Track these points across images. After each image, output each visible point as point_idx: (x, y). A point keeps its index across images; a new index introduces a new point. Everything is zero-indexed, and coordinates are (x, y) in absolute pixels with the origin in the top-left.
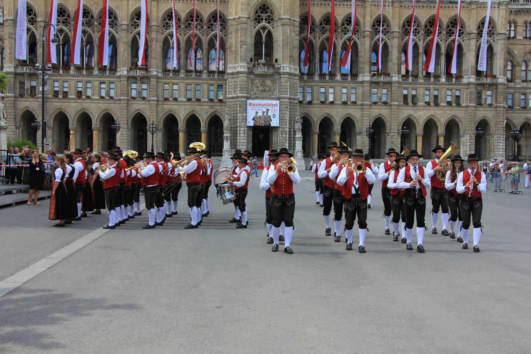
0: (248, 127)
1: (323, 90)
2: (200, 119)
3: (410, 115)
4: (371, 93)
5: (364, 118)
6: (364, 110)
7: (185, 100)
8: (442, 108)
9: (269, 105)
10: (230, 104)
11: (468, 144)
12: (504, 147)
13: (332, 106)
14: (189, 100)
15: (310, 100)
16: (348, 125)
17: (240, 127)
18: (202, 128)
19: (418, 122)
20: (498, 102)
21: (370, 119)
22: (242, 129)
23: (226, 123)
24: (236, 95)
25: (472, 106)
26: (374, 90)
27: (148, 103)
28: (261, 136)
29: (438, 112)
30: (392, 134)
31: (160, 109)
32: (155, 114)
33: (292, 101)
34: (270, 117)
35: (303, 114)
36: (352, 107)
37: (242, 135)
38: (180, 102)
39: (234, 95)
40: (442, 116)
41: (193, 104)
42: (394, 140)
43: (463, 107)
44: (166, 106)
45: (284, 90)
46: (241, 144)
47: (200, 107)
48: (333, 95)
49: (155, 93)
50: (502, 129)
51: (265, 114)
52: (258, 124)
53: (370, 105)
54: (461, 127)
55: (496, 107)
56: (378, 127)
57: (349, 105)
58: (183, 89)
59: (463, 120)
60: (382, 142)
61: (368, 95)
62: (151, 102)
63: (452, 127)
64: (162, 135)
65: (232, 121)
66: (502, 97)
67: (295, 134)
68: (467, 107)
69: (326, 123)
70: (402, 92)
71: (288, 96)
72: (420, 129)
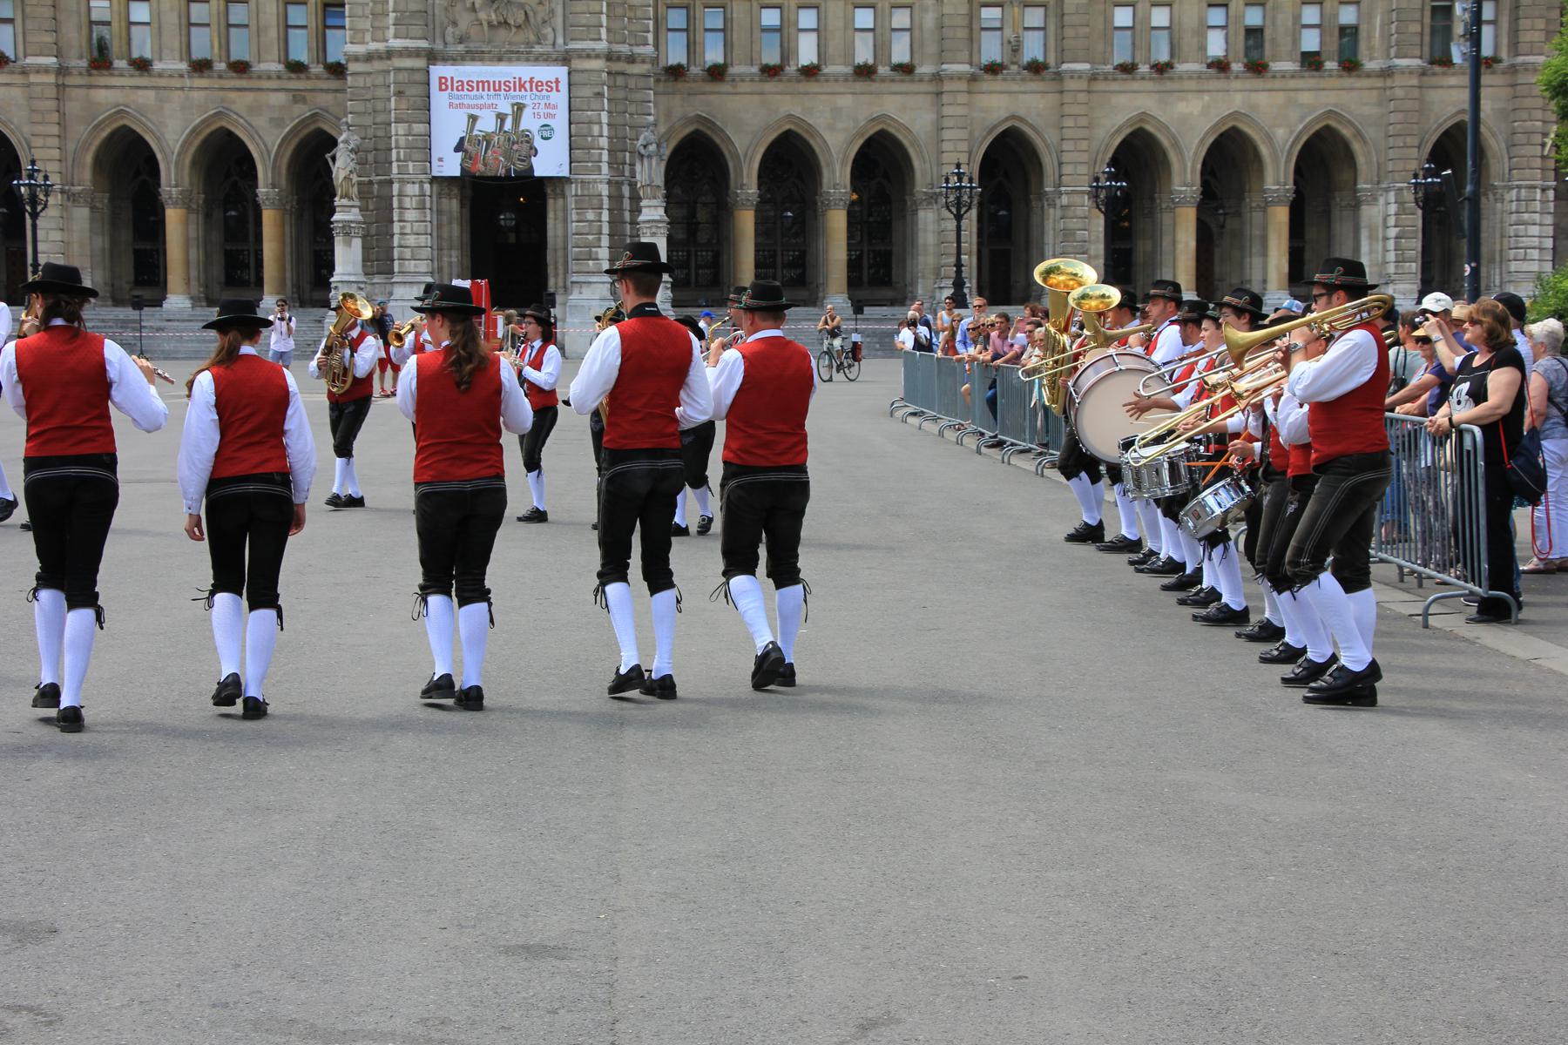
0: (435, 180)
1: (771, 18)
2: (251, 147)
3: (1143, 117)
4: (973, 29)
5: (946, 135)
6: (945, 98)
7: (184, 66)
8: (1277, 84)
9: (522, 86)
10: (360, 81)
11: (1392, 232)
12: (1549, 243)
13: (812, 86)
14: (201, 67)
15: (721, 60)
16: (882, 162)
17: (402, 181)
18: (262, 190)
19: (1176, 145)
20: (1522, 47)
21: (970, 140)
22: (413, 189)
23: (342, 166)
24: (381, 46)
25: (1410, 71)
26: (987, 13)
27: (18, 79)
28: (506, 219)
29: (1262, 99)
30: (1065, 200)
31: (73, 107)
32: (55, 130)
33: (617, 67)
34: (527, 138)
35: (690, 121)
36: (896, 87)
37: (411, 215)
38: (160, 75)
39: (373, 46)
40: (1279, 117)
41: (217, 83)
42: (1073, 224)
43: (1368, 75)
44: (101, 96)
45: (583, 19)
46: (408, 253)
47: (249, 97)
48: (814, 36)
49: (49, 38)
50: (1538, 162)
51: (508, 125)
52: (480, 167)
53: (973, 79)
54: (1361, 160)
55: (1513, 69)
56: (1009, 168)
57: (883, 80)
58: (171, 19)
59: (1370, 133)
60: (1035, 233)
61: (962, 33)
62: (33, 78)
63: (1324, 162)
64: (92, 220)
65: (371, 158)
66: (1541, 24)
67: (637, 210)
68: (1387, 73)
69: (790, 159)
70: (1108, 18)
71: (602, 46)
72: (1185, 178)
